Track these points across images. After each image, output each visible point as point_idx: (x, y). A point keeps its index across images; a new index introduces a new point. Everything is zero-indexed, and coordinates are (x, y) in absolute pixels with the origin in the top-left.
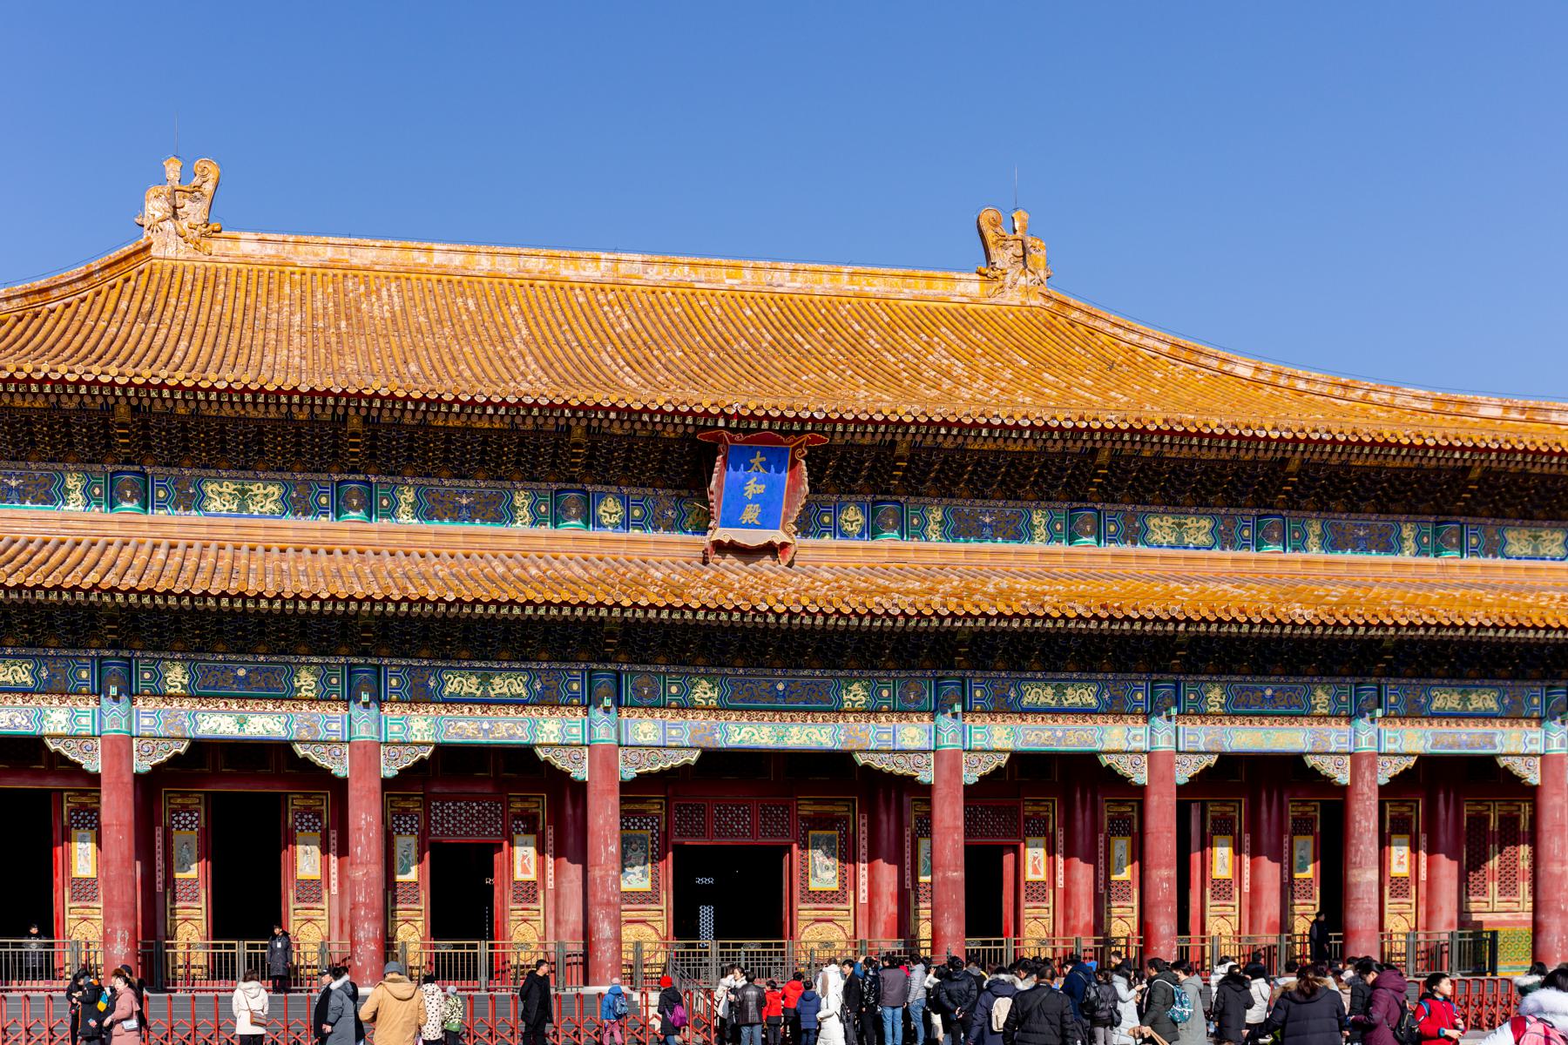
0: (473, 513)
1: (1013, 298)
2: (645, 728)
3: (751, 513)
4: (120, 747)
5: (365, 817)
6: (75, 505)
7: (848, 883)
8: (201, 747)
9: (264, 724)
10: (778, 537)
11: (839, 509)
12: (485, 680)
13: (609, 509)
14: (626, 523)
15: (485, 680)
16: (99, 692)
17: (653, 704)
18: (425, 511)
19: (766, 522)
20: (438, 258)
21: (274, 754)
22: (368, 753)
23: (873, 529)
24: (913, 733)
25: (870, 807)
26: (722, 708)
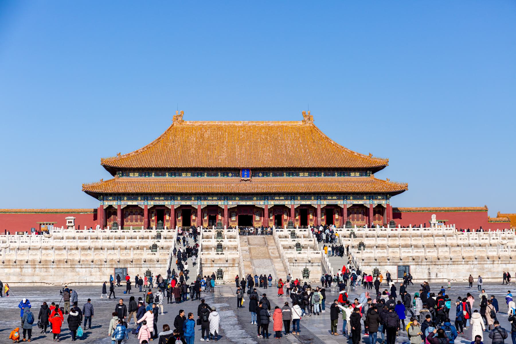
0: (214, 176)
1: (308, 125)
2: (230, 203)
3: (246, 176)
4: (173, 206)
5: (199, 213)
6: (167, 176)
7: (260, 219)
8: (182, 206)
9: (188, 203)
10: (249, 178)
12: (213, 198)
13: (230, 174)
14: (232, 176)
15: (213, 198)
16: (171, 200)
17: (231, 200)
18: (208, 176)
19: (248, 177)
20: (216, 123)
21: (190, 206)
22: (199, 206)
23: (263, 176)
24: (262, 203)
25: (260, 211)
26: (239, 200)
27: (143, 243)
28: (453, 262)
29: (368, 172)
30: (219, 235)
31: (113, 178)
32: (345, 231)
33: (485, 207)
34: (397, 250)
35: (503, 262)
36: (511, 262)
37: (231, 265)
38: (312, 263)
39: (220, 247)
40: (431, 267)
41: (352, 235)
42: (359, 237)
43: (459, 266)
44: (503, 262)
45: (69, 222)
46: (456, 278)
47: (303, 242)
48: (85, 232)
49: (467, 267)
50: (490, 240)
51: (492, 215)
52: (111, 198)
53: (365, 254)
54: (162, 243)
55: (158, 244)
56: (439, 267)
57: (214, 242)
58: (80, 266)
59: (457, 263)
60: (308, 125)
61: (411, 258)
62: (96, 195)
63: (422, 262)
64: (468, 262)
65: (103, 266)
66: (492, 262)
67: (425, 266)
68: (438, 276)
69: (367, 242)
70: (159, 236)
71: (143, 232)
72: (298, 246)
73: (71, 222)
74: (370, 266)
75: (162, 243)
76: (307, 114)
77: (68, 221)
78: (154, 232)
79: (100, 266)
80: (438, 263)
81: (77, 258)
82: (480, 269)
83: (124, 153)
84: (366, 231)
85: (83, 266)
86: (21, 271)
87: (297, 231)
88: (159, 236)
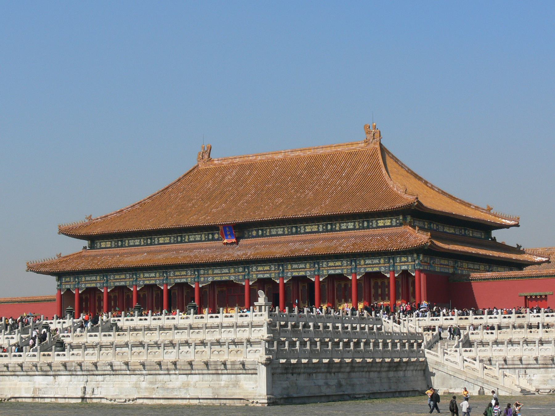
11: (253, 230)
28: (113, 371)
35: (182, 372)
36: (193, 372)
40: (90, 378)
41: (114, 328)
43: (125, 376)
44: (182, 372)
46: (115, 397)
52: (68, 279)
56: (100, 378)
59: (120, 372)
60: (372, 145)
64: (134, 370)
66: (166, 372)
68: (95, 392)
74: (18, 376)
80: (97, 373)
82: (151, 383)
83: (97, 215)
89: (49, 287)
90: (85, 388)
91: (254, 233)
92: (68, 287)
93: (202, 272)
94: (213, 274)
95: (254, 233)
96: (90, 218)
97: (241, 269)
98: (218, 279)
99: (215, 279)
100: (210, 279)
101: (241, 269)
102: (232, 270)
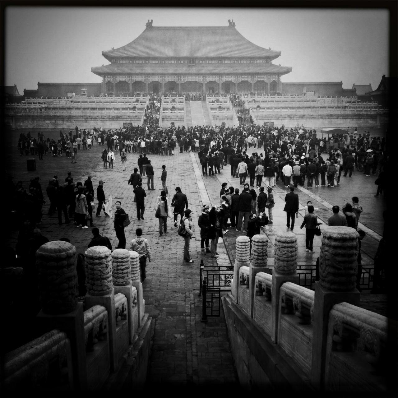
10: (194, 65)
27: (127, 105)
29: (268, 60)
30: (174, 100)
31: (110, 63)
32: (250, 98)
33: (341, 82)
34: (279, 110)
37: (180, 119)
38: (228, 118)
39: (173, 109)
40: (299, 120)
42: (257, 102)
45: (83, 92)
47: (223, 105)
48: (93, 99)
49: (321, 120)
50: (338, 103)
51: (344, 87)
52: (109, 77)
53: (261, 112)
54: (139, 105)
55: (137, 106)
57: (170, 106)
58: (90, 119)
61: (287, 115)
62: (100, 74)
63: (293, 117)
65: (104, 119)
67: (296, 120)
69: (262, 105)
70: (137, 101)
71: (128, 99)
72: (220, 108)
73: (84, 92)
74: (262, 120)
75: (139, 105)
76: (231, 21)
77: (82, 91)
78: (134, 99)
79: (102, 120)
81: (88, 115)
84: (262, 98)
85: (92, 119)
86: (55, 122)
87: (221, 99)
88: (137, 101)
89: (99, 80)
90: (298, 124)
91: (201, 62)
92: (109, 80)
93: (182, 77)
94: (188, 78)
95: (201, 62)
96: (113, 49)
97: (201, 77)
98: (191, 80)
99: (189, 80)
100: (186, 80)
101: (201, 77)
102: (197, 77)
